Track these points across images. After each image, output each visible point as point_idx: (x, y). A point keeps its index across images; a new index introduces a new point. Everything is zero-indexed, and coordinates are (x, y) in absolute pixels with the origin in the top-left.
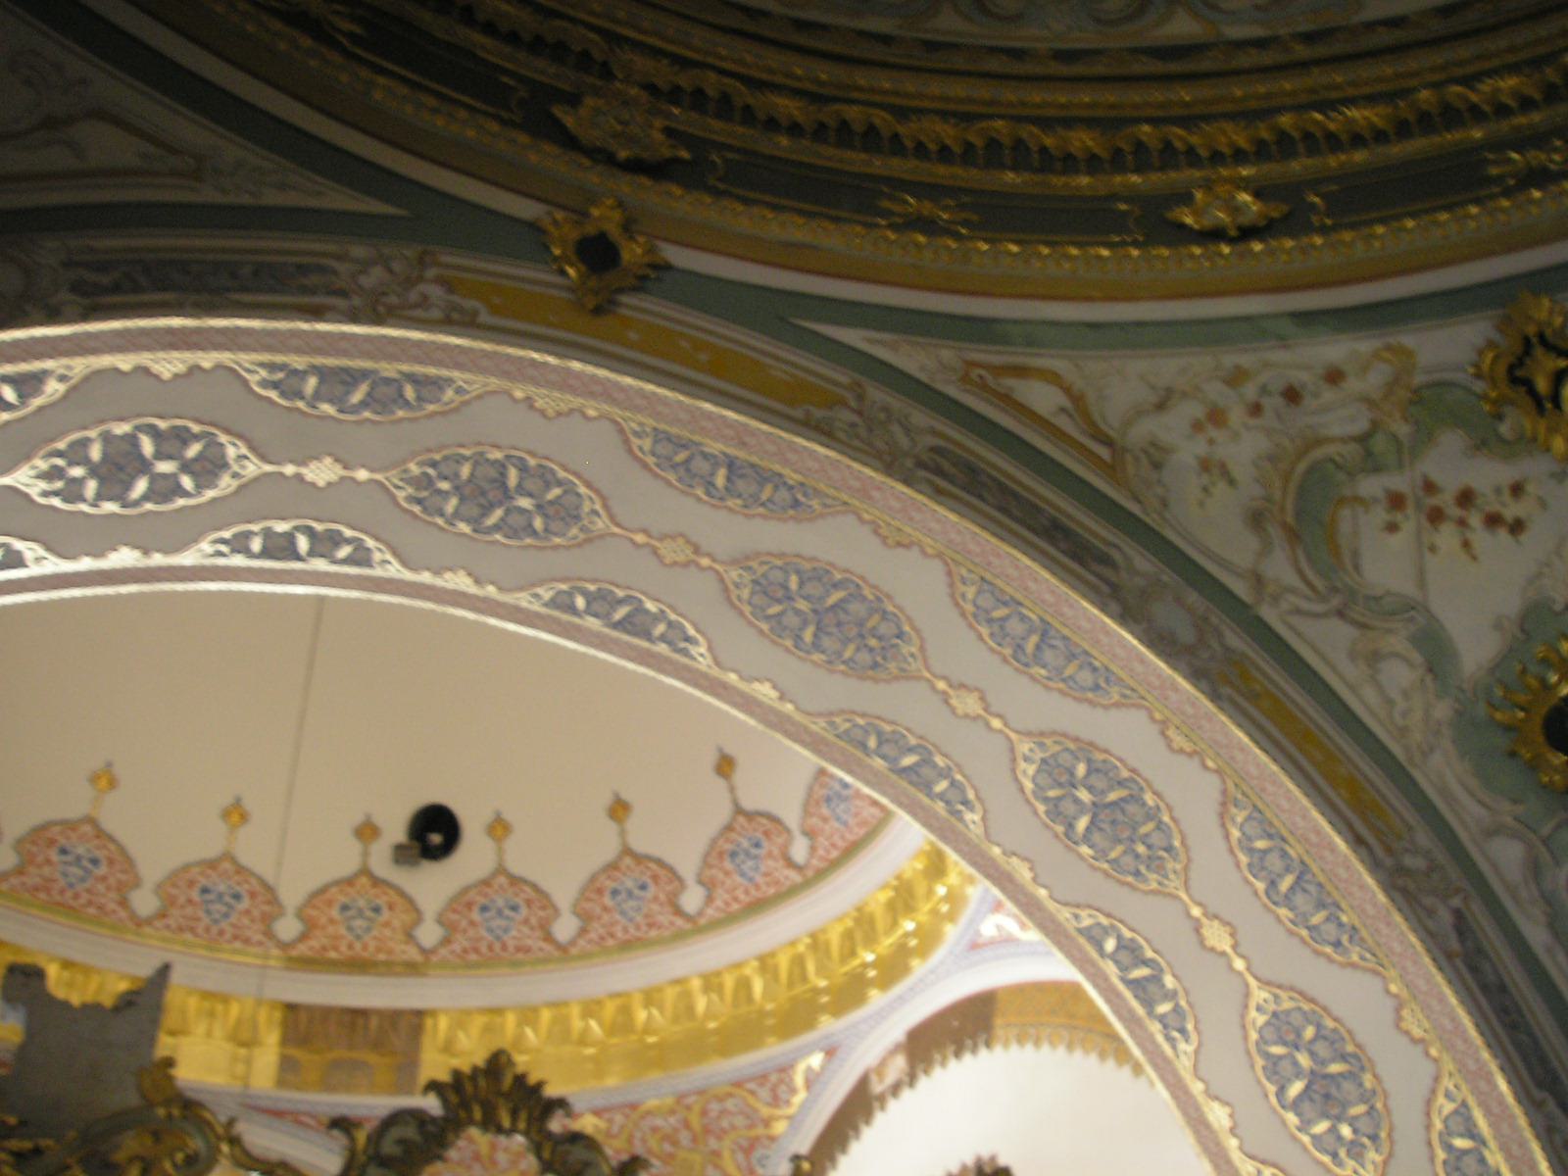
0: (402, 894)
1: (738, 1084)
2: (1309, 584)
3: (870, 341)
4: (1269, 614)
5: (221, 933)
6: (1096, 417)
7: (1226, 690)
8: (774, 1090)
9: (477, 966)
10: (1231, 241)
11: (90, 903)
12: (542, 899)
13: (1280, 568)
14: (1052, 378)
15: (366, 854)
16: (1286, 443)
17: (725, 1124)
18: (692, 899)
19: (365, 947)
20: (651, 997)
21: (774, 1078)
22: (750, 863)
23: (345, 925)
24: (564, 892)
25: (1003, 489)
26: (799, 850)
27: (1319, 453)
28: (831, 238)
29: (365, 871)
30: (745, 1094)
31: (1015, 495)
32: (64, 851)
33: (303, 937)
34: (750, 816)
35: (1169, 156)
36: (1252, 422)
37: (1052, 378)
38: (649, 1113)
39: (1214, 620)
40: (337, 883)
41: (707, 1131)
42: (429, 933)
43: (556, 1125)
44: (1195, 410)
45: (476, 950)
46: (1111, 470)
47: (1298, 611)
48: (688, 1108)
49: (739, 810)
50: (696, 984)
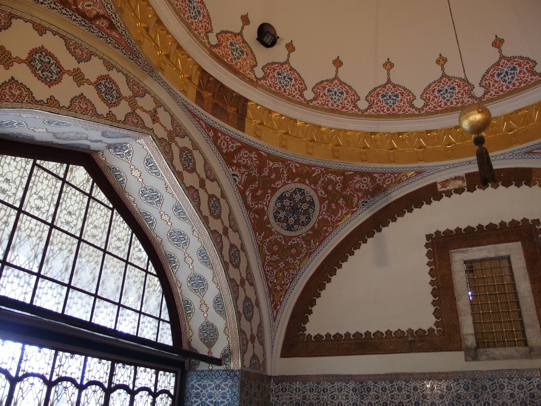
0: (252, 52)
8: (384, 180)
15: (242, 28)
19: (236, 64)
29: (240, 34)
40: (231, 33)
45: (275, 87)
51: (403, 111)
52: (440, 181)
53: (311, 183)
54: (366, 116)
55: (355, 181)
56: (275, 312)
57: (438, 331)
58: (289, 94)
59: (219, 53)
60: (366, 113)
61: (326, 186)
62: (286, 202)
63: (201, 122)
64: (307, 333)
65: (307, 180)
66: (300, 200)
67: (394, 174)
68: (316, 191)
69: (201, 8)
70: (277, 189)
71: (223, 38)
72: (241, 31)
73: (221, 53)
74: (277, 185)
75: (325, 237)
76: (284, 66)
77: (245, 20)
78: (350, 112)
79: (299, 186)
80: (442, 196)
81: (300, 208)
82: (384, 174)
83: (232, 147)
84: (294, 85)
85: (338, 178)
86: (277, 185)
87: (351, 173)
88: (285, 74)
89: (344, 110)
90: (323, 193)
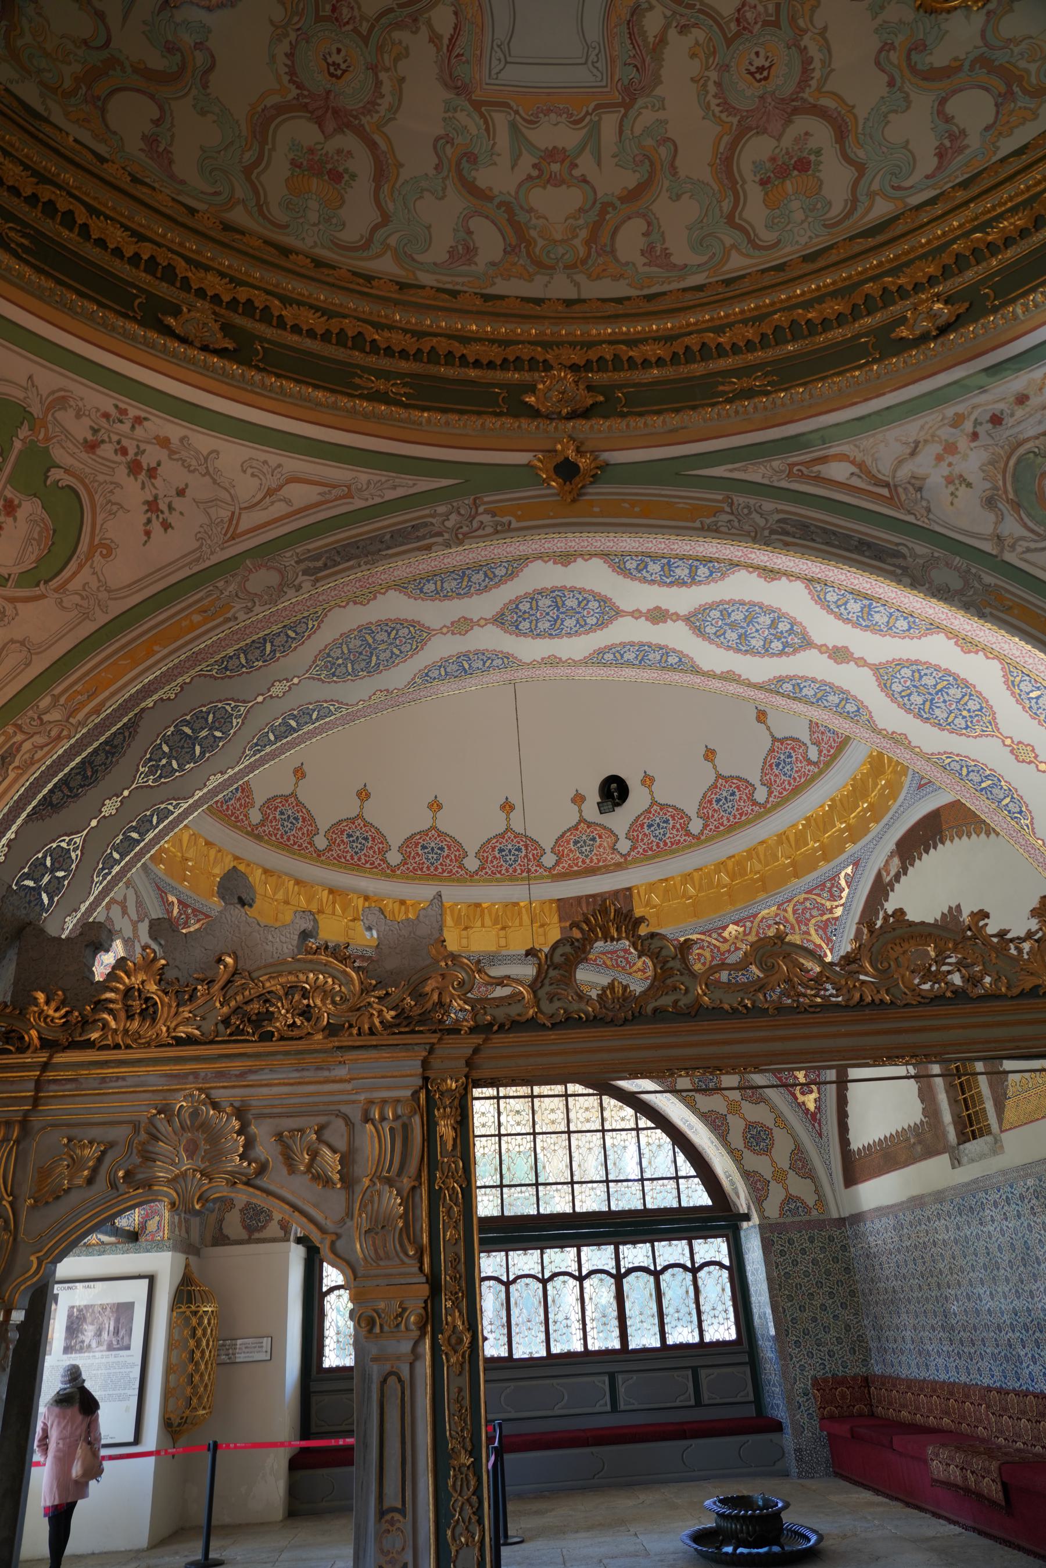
0: (605, 828)
1: (809, 892)
2: (1032, 531)
3: (731, 471)
4: (1010, 557)
6: (874, 471)
7: (987, 610)
8: (830, 891)
9: (653, 857)
10: (936, 337)
13: (1011, 527)
14: (843, 457)
15: (580, 811)
16: (998, 450)
17: (808, 915)
18: (761, 794)
21: (828, 885)
23: (578, 851)
24: (691, 808)
25: (825, 531)
26: (813, 754)
27: (1021, 450)
28: (693, 419)
29: (582, 820)
31: (834, 533)
32: (424, 847)
34: (782, 741)
35: (887, 297)
36: (973, 445)
37: (843, 457)
39: (973, 571)
40: (569, 830)
42: (624, 846)
43: (643, 930)
44: (938, 448)
45: (651, 849)
46: (890, 501)
47: (1028, 550)
49: (775, 739)
54: (769, 811)
67: (833, 879)
77: (578, 799)
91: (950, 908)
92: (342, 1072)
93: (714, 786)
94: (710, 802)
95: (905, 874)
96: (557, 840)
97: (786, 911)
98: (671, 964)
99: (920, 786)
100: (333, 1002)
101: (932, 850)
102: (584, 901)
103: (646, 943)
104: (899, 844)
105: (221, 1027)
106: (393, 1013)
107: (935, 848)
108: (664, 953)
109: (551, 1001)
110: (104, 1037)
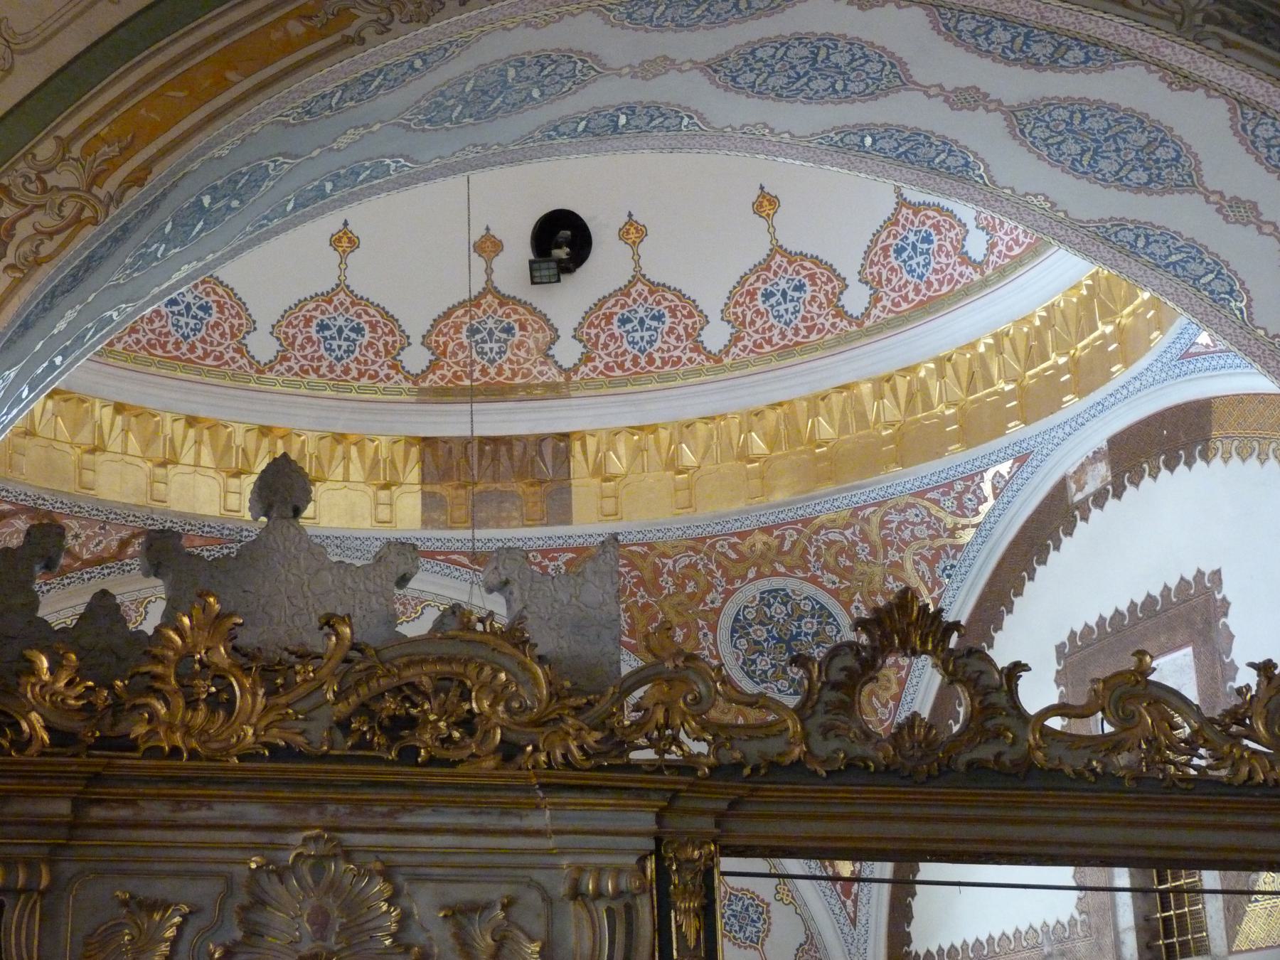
0: (533, 311)
1: (921, 494)
5: (346, 371)
8: (959, 498)
11: (206, 355)
12: (688, 306)
15: (489, 271)
17: (906, 535)
18: (856, 299)
20: (817, 401)
21: (959, 487)
22: (920, 259)
24: (711, 300)
29: (490, 289)
30: (927, 503)
33: (432, 367)
38: (822, 527)
40: (461, 304)
41: (886, 543)
42: (568, 351)
45: (621, 366)
48: (867, 520)
50: (866, 388)
51: (950, 282)
52: (1072, 471)
53: (791, 569)
54: (869, 333)
55: (894, 525)
56: (849, 903)
57: (1083, 922)
58: (665, 363)
59: (443, 377)
60: (868, 323)
61: (831, 561)
62: (755, 631)
63: (454, 557)
64: (913, 948)
65: (777, 565)
66: (787, 614)
67: (971, 477)
68: (814, 580)
69: (359, 316)
70: (718, 612)
71: (445, 335)
72: (489, 280)
73: (450, 375)
74: (712, 602)
75: (902, 683)
76: (633, 291)
77: (488, 246)
78: (829, 336)
79: (765, 584)
80: (1075, 517)
81: (799, 634)
82: (950, 486)
83: (557, 568)
84: (671, 330)
85: (848, 533)
86: (712, 602)
87: (872, 509)
88: (641, 313)
89: (814, 337)
90: (835, 578)
91: (1200, 574)
92: (542, 820)
93: (765, 265)
94: (752, 294)
95: (1118, 495)
96: (436, 321)
97: (867, 520)
98: (994, 698)
99: (1186, 355)
100: (508, 709)
101: (1182, 468)
102: (474, 450)
103: (960, 661)
104: (1114, 442)
105: (338, 735)
106: (598, 735)
107: (1189, 464)
108: (984, 680)
109: (825, 738)
110: (152, 733)
